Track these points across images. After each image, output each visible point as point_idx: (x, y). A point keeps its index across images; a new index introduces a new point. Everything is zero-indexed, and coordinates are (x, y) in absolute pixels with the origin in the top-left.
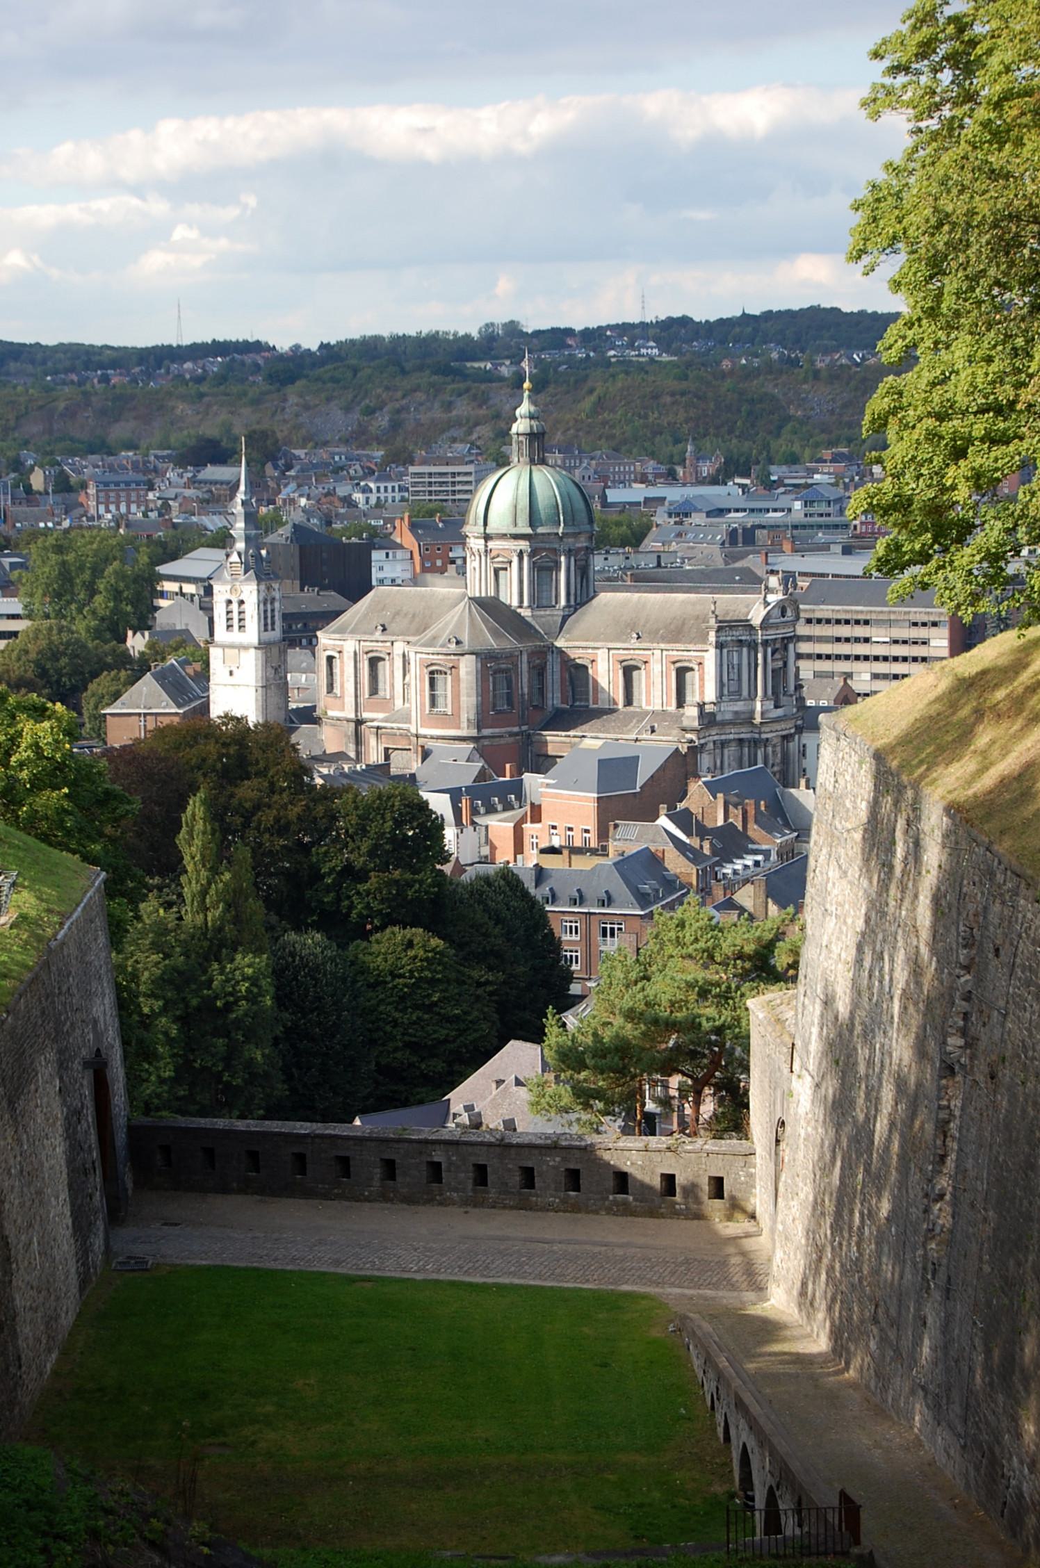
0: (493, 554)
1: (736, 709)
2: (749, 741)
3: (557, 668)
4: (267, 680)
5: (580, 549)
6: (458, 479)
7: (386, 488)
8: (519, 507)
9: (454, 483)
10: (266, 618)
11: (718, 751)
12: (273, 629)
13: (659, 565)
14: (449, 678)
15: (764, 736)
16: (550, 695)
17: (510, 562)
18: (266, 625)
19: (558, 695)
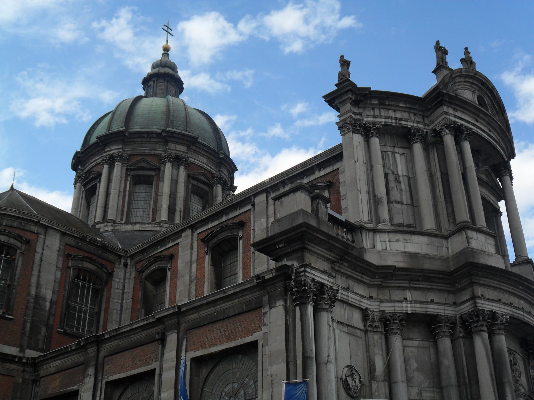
1: (411, 248)
2: (452, 323)
3: (130, 286)
11: (376, 338)
15: (485, 306)
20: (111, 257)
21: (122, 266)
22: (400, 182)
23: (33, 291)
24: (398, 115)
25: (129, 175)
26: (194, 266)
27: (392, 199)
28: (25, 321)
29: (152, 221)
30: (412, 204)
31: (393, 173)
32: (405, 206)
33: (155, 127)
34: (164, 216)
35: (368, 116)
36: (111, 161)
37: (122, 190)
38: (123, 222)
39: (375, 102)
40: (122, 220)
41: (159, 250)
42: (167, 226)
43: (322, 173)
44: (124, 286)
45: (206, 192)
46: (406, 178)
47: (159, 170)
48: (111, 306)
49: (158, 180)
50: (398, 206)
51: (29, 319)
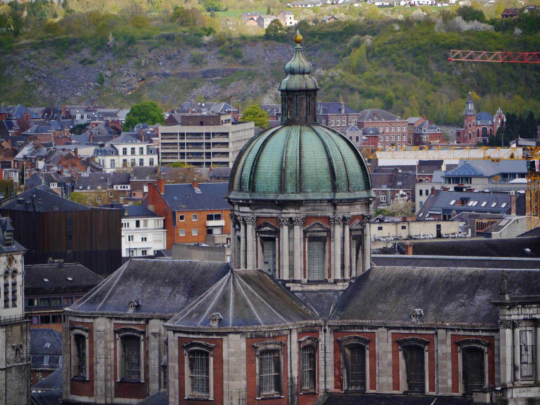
0: (261, 222)
3: (330, 348)
4: (7, 362)
5: (354, 217)
6: (212, 140)
7: (133, 150)
8: (289, 171)
9: (208, 145)
10: (6, 293)
12: (14, 306)
13: (439, 235)
14: (211, 359)
16: (322, 379)
17: (277, 232)
18: (6, 301)
19: (331, 379)
20: (317, 328)
21: (323, 332)
22: (527, 350)
23: (289, 376)
24: (531, 311)
25: (306, 237)
26: (390, 356)
27: (523, 361)
28: (288, 396)
29: (329, 278)
30: (533, 363)
31: (524, 345)
32: (529, 365)
33: (324, 190)
34: (339, 277)
35: (515, 315)
36: (291, 222)
37: (302, 251)
38: (306, 280)
39: (520, 306)
40: (305, 277)
41: (357, 331)
42: (341, 284)
43: (484, 334)
44: (325, 348)
45: (360, 236)
46: (531, 347)
47: (329, 231)
48: (320, 364)
49: (330, 241)
50: (525, 365)
51: (289, 394)
